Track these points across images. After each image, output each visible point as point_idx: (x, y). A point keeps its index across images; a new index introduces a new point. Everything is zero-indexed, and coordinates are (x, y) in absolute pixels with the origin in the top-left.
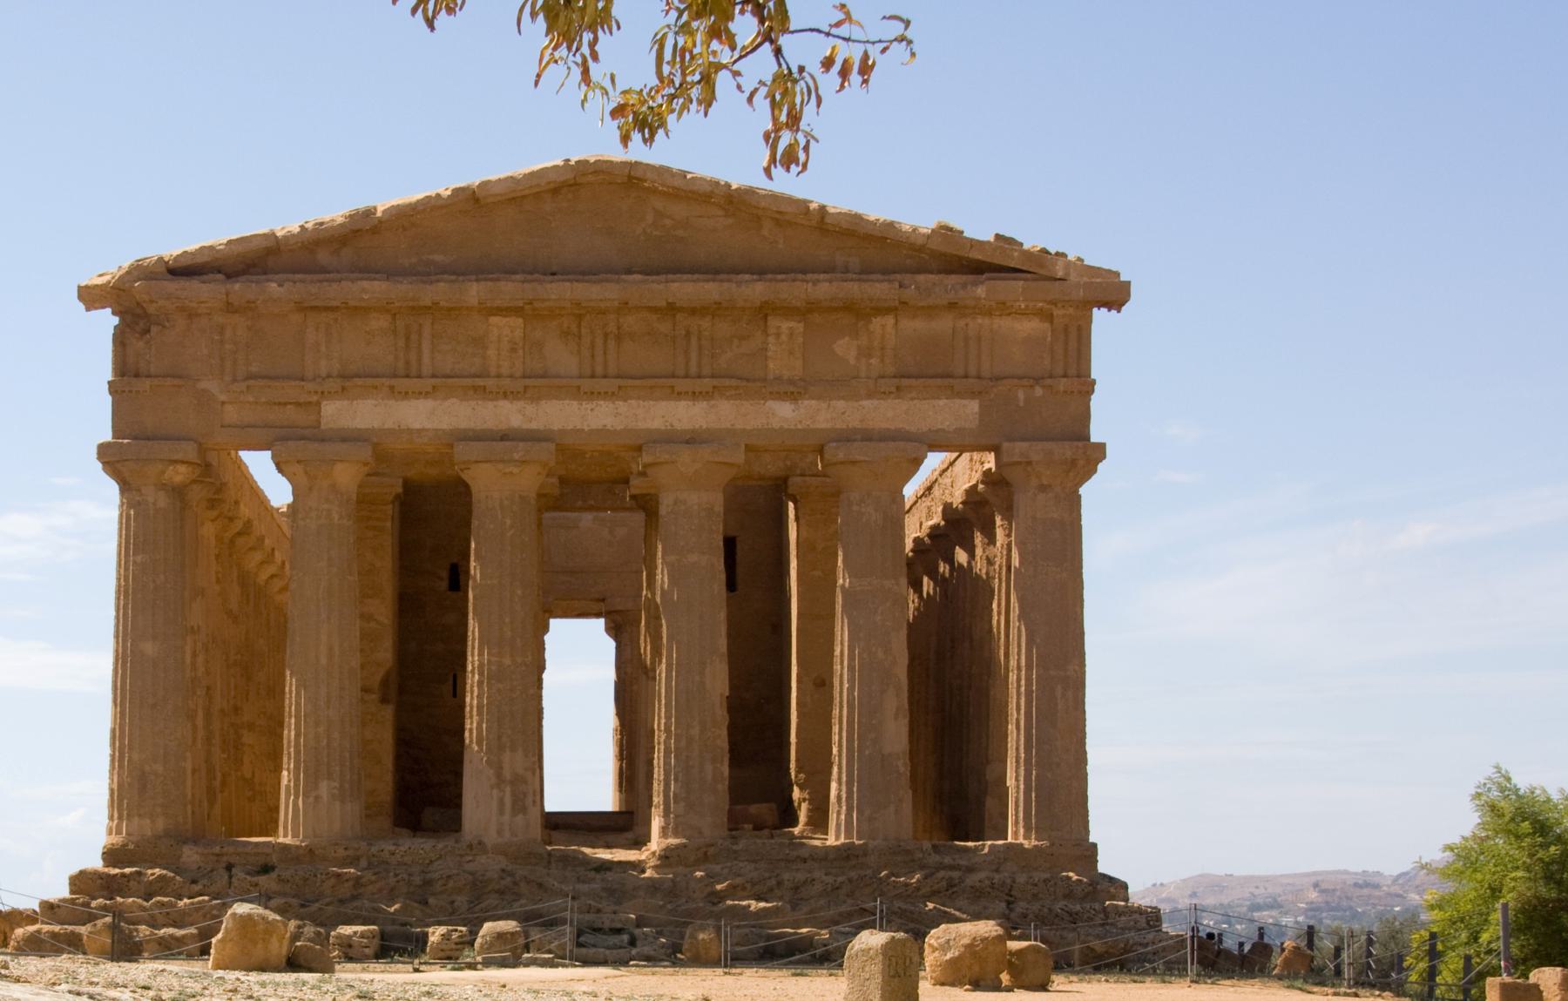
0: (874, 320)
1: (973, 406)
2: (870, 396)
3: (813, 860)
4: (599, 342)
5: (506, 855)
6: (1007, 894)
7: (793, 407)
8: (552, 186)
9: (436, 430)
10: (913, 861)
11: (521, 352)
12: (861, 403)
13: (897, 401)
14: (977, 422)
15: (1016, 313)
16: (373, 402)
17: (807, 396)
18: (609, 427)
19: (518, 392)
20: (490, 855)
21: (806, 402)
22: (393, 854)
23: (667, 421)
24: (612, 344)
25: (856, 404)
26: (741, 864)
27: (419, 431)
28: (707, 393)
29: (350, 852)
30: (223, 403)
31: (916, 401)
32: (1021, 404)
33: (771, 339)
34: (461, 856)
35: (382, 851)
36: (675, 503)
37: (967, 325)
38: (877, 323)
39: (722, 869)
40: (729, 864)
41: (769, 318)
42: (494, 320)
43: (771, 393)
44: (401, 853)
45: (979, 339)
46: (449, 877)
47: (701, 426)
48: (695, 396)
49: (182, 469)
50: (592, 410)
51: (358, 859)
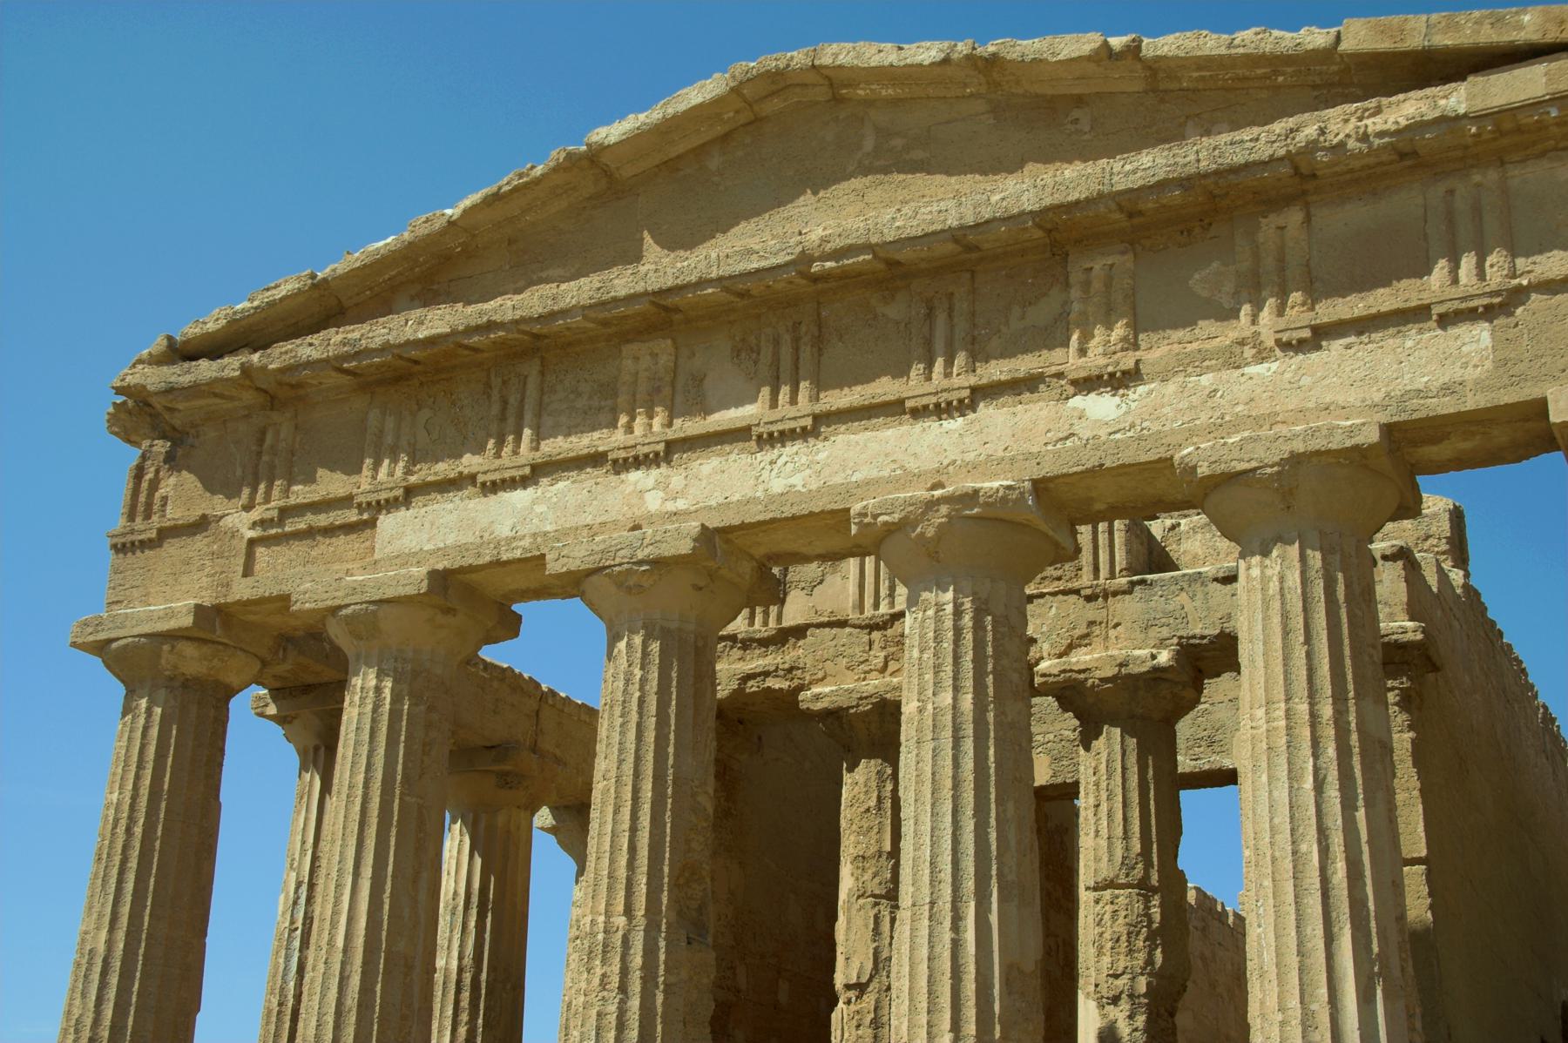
0: (1263, 221)
1: (1480, 336)
2: (1262, 356)
4: (786, 352)
7: (1117, 399)
8: (720, 130)
9: (534, 535)
11: (667, 391)
12: (1247, 370)
14: (1488, 364)
15: (1556, 149)
16: (450, 506)
18: (799, 488)
19: (657, 454)
21: (1141, 389)
24: (806, 353)
27: (510, 540)
28: (961, 401)
30: (252, 543)
31: (1352, 351)
33: (1075, 293)
37: (1451, 192)
38: (1268, 226)
41: (1070, 258)
42: (628, 349)
43: (1074, 383)
45: (1477, 211)
48: (942, 411)
49: (189, 649)
50: (772, 463)
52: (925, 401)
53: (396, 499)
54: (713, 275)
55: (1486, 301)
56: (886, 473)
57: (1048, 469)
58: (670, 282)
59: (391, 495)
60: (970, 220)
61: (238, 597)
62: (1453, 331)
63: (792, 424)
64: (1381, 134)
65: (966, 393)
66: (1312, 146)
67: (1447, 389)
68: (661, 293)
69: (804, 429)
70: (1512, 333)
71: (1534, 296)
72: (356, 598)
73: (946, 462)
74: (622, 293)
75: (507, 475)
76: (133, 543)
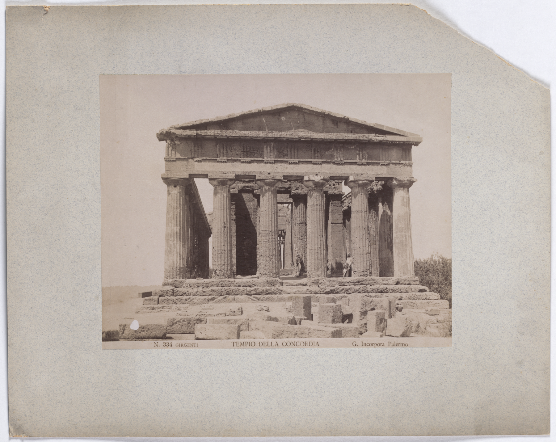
6: (400, 291)
19: (273, 162)
28: (320, 163)
29: (230, 283)
46: (257, 289)
52: (315, 162)
53: (225, 161)
54: (286, 137)
55: (386, 164)
57: (332, 175)
58: (279, 137)
59: (224, 160)
60: (326, 138)
61: (194, 173)
62: (382, 166)
63: (295, 162)
64: (378, 140)
65: (321, 162)
66: (371, 139)
68: (277, 137)
69: (297, 163)
70: (389, 168)
71: (391, 164)
72: (221, 178)
74: (270, 136)
75: (246, 161)
76: (170, 160)
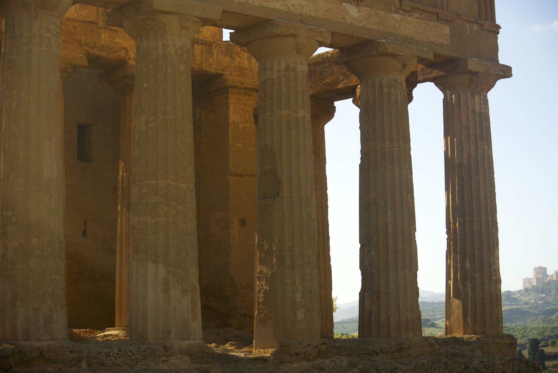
1: (447, 30)
2: (397, 12)
3: (382, 352)
5: (190, 356)
10: (434, 351)
13: (410, 18)
17: (364, 4)
20: (179, 356)
21: (364, 8)
22: (108, 356)
23: (286, 5)
25: (390, 15)
26: (342, 358)
32: (468, 33)
34: (160, 356)
35: (100, 353)
36: (287, 69)
39: (330, 362)
40: (333, 358)
44: (115, 356)
47: (306, 13)
51: (80, 360)
56: (282, 8)
67: (441, 45)
73: (304, 12)
